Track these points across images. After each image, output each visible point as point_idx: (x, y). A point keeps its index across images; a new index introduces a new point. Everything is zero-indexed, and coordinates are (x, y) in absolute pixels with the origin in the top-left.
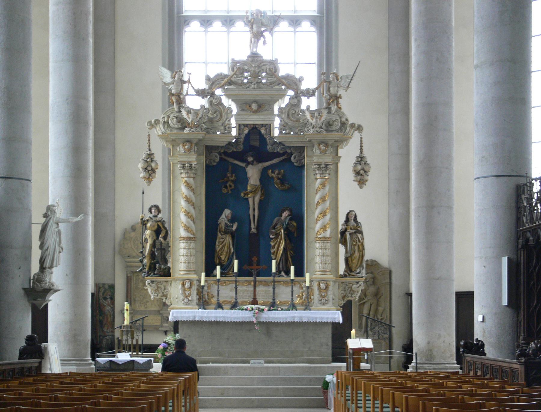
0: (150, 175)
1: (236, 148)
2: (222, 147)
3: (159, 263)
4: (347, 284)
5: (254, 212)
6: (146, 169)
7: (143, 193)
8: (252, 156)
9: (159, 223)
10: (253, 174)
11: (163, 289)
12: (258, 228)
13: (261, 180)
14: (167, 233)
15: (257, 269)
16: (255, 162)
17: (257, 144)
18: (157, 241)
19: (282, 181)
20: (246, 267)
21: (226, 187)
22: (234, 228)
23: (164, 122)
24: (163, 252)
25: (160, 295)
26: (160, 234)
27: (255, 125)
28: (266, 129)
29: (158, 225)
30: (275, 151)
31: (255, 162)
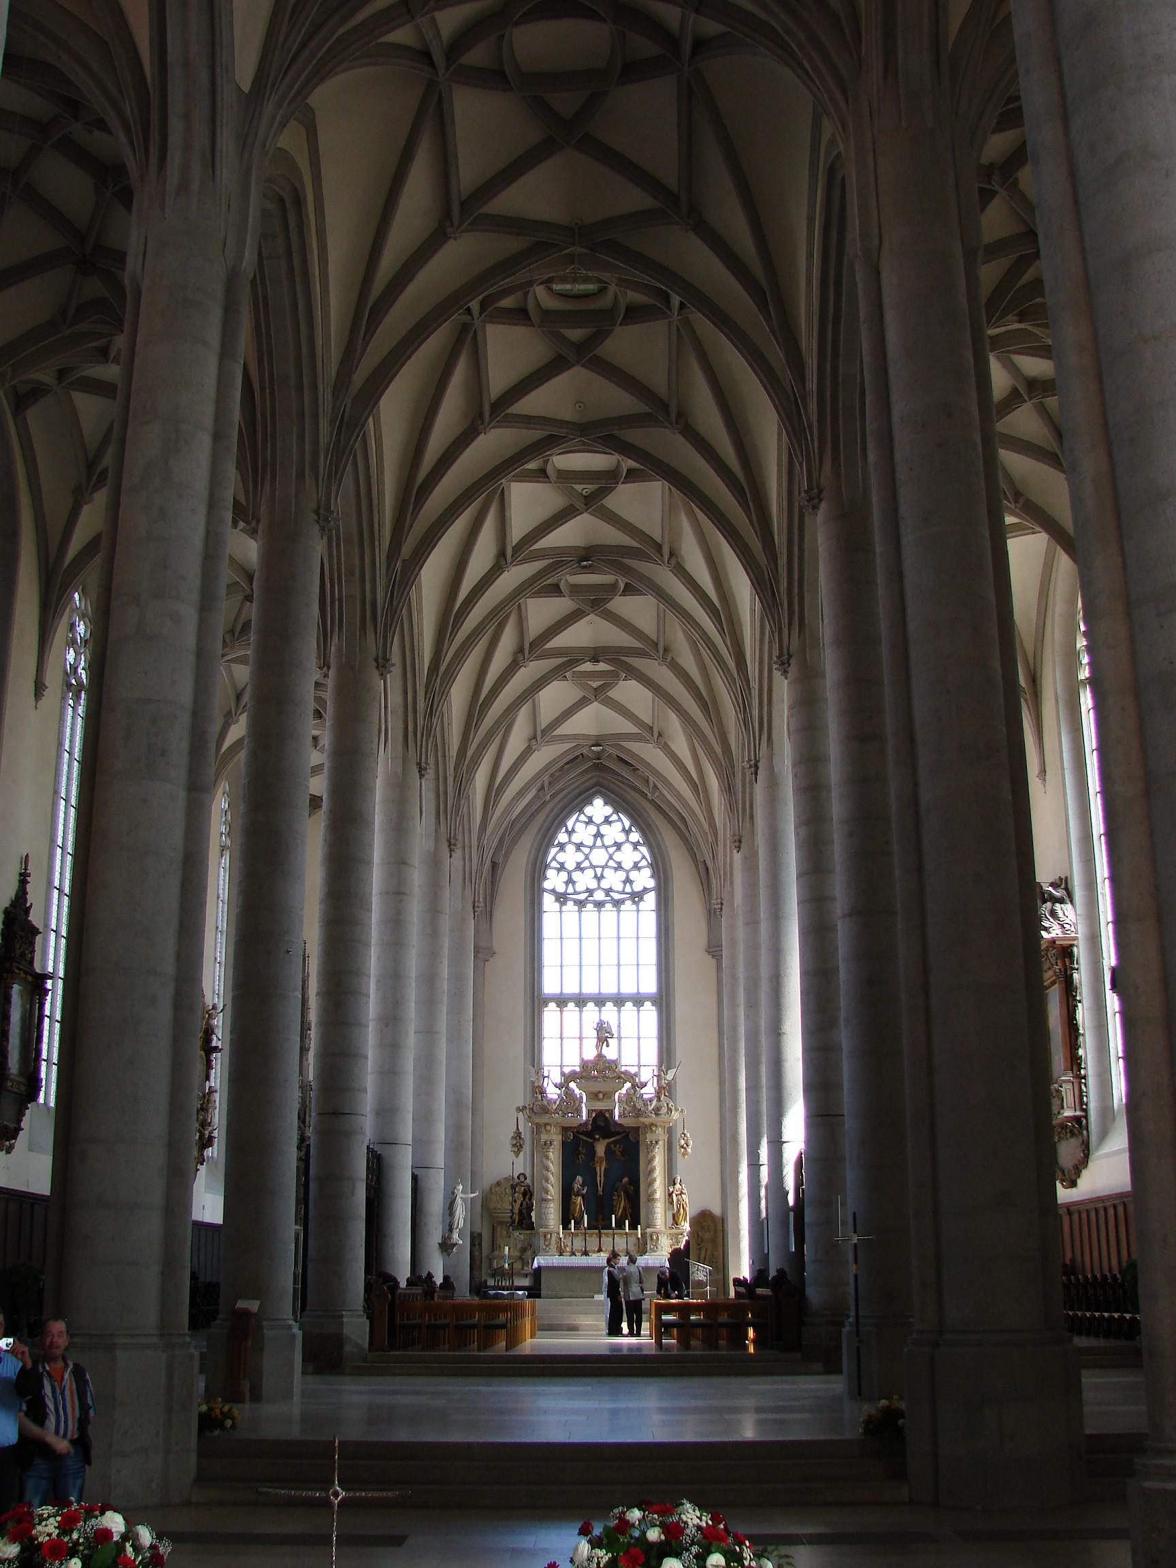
3: (524, 1221)
5: (600, 1179)
10: (600, 1148)
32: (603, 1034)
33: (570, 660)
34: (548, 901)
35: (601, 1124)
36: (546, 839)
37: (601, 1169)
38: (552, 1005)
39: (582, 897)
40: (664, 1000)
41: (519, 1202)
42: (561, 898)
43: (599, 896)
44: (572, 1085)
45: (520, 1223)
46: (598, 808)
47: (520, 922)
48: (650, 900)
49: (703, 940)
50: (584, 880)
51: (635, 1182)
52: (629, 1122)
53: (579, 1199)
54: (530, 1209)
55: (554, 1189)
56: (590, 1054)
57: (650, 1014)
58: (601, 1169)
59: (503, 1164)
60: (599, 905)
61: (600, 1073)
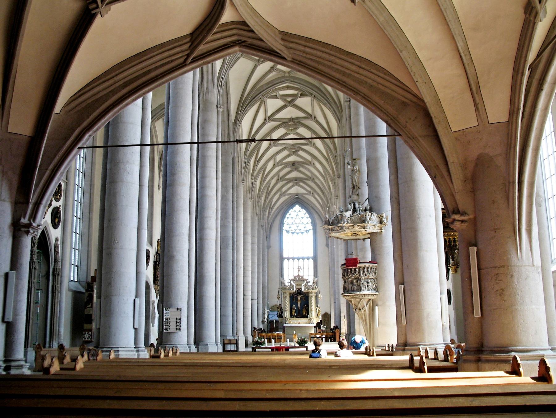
5: (299, 305)
10: (299, 298)
32: (299, 269)
33: (290, 180)
34: (284, 233)
35: (299, 292)
36: (283, 217)
37: (299, 303)
38: (286, 260)
39: (293, 231)
40: (315, 258)
42: (288, 232)
43: (298, 231)
44: (292, 282)
46: (297, 206)
47: (277, 238)
48: (311, 232)
49: (325, 242)
50: (294, 227)
51: (308, 306)
52: (306, 291)
54: (282, 313)
55: (288, 308)
56: (296, 274)
57: (311, 262)
58: (299, 303)
59: (276, 302)
60: (298, 233)
61: (299, 279)
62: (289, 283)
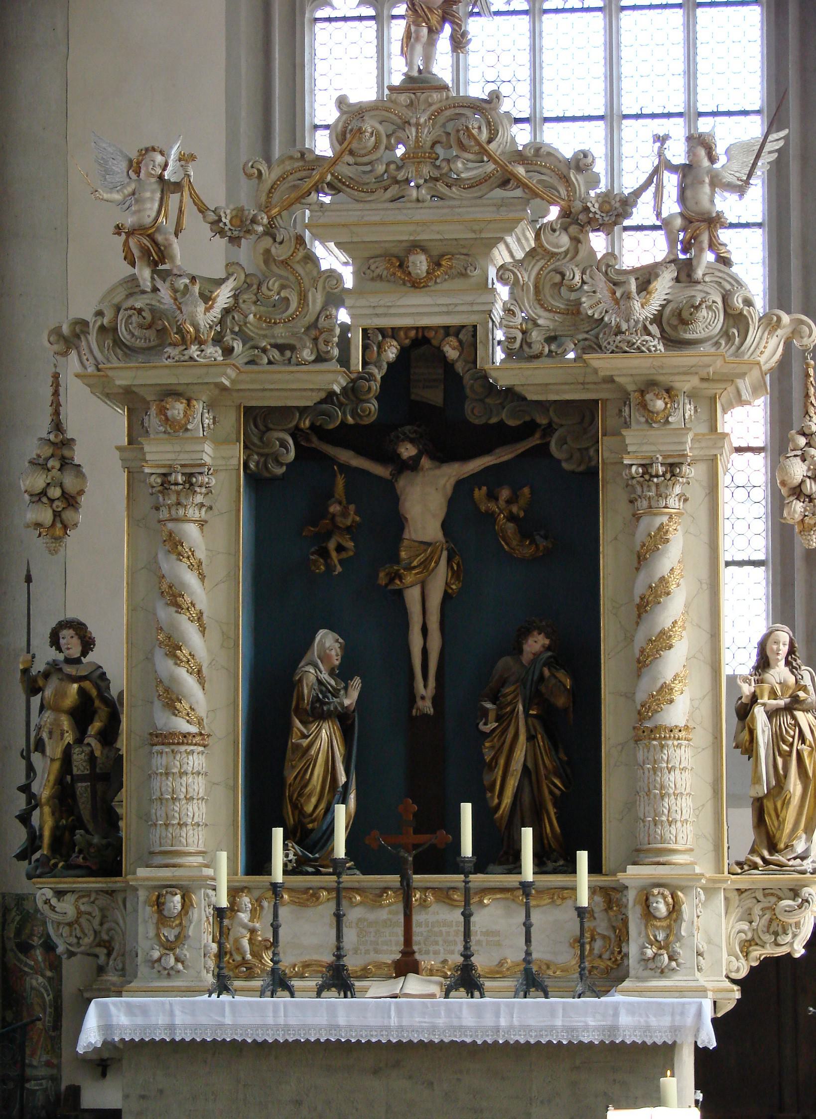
0: (57, 515)
1: (354, 414)
2: (303, 410)
4: (760, 896)
5: (424, 641)
6: (43, 493)
7: (29, 579)
8: (412, 441)
9: (87, 685)
11: (96, 922)
12: (437, 700)
13: (445, 526)
14: (114, 720)
15: (415, 846)
16: (425, 462)
17: (435, 396)
18: (76, 750)
19: (526, 528)
20: (378, 840)
21: (324, 553)
22: (350, 700)
23: (102, 328)
24: (100, 787)
25: (87, 941)
26: (91, 721)
27: (424, 328)
28: (460, 342)
29: (82, 691)
30: (494, 420)
31: (425, 462)
41: (55, 749)
45: (61, 843)
51: (579, 655)
53: (325, 738)
54: (108, 776)
58: (425, 596)
62: (235, 229)
